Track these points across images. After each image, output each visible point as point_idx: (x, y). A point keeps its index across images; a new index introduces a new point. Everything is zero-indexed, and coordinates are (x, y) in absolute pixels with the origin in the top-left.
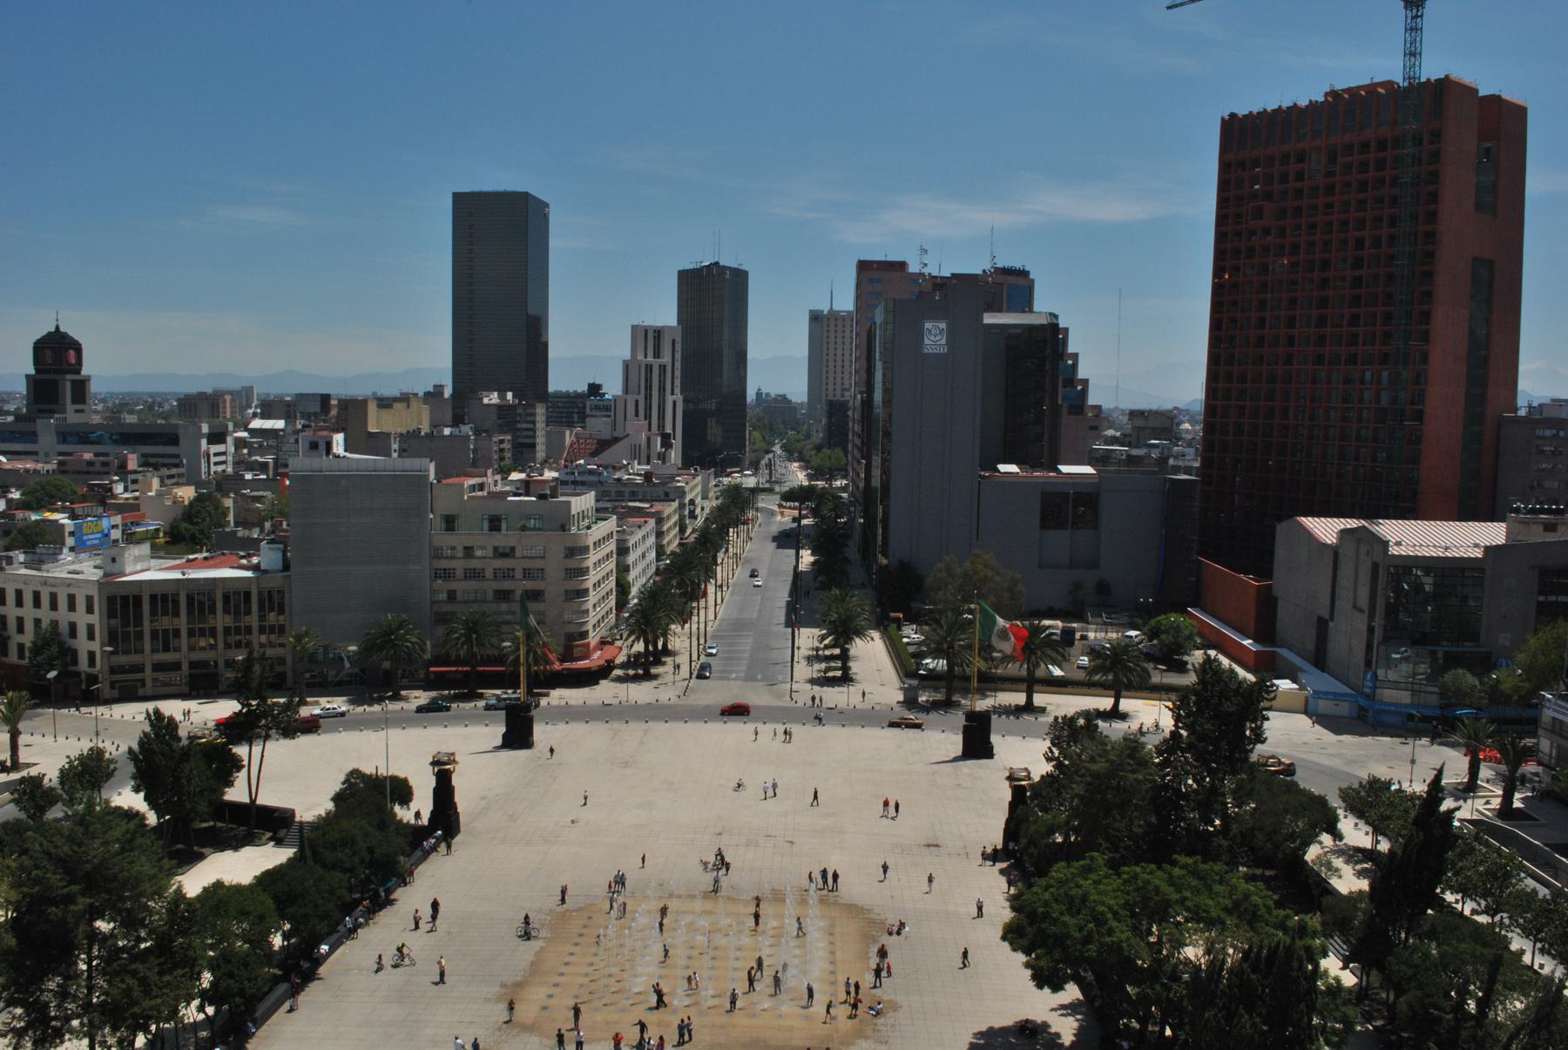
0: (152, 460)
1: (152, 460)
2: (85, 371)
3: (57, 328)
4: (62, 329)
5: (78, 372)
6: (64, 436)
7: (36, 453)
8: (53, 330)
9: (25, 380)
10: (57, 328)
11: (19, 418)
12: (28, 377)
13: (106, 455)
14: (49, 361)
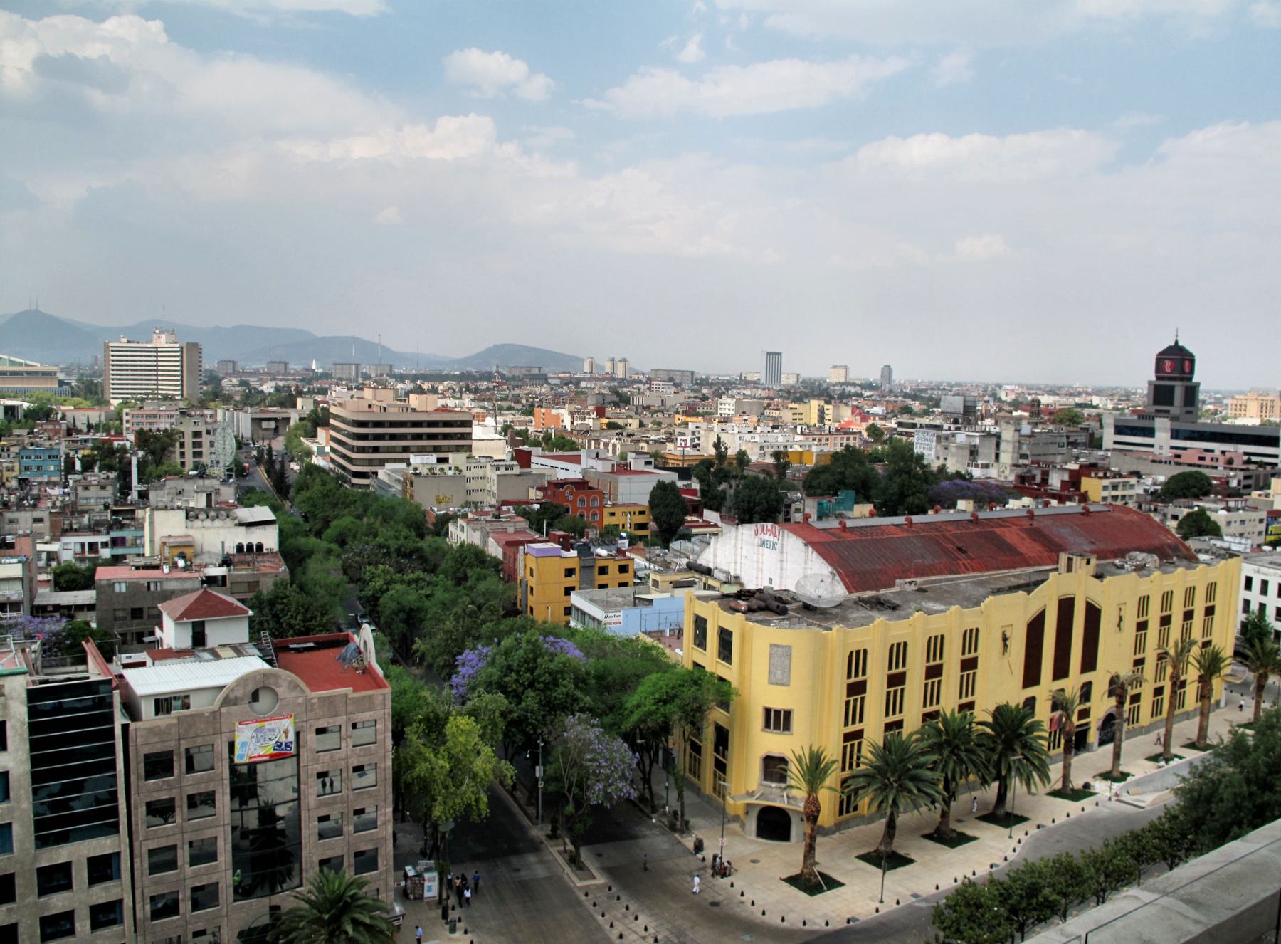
0: (1254, 459)
1: (1254, 459)
2: (1195, 380)
3: (1176, 342)
4: (1180, 344)
5: (1190, 379)
6: (1175, 434)
7: (1152, 446)
8: (1172, 344)
9: (1147, 386)
10: (1176, 342)
11: (1142, 416)
12: (1150, 383)
13: (1212, 451)
14: (1168, 370)
